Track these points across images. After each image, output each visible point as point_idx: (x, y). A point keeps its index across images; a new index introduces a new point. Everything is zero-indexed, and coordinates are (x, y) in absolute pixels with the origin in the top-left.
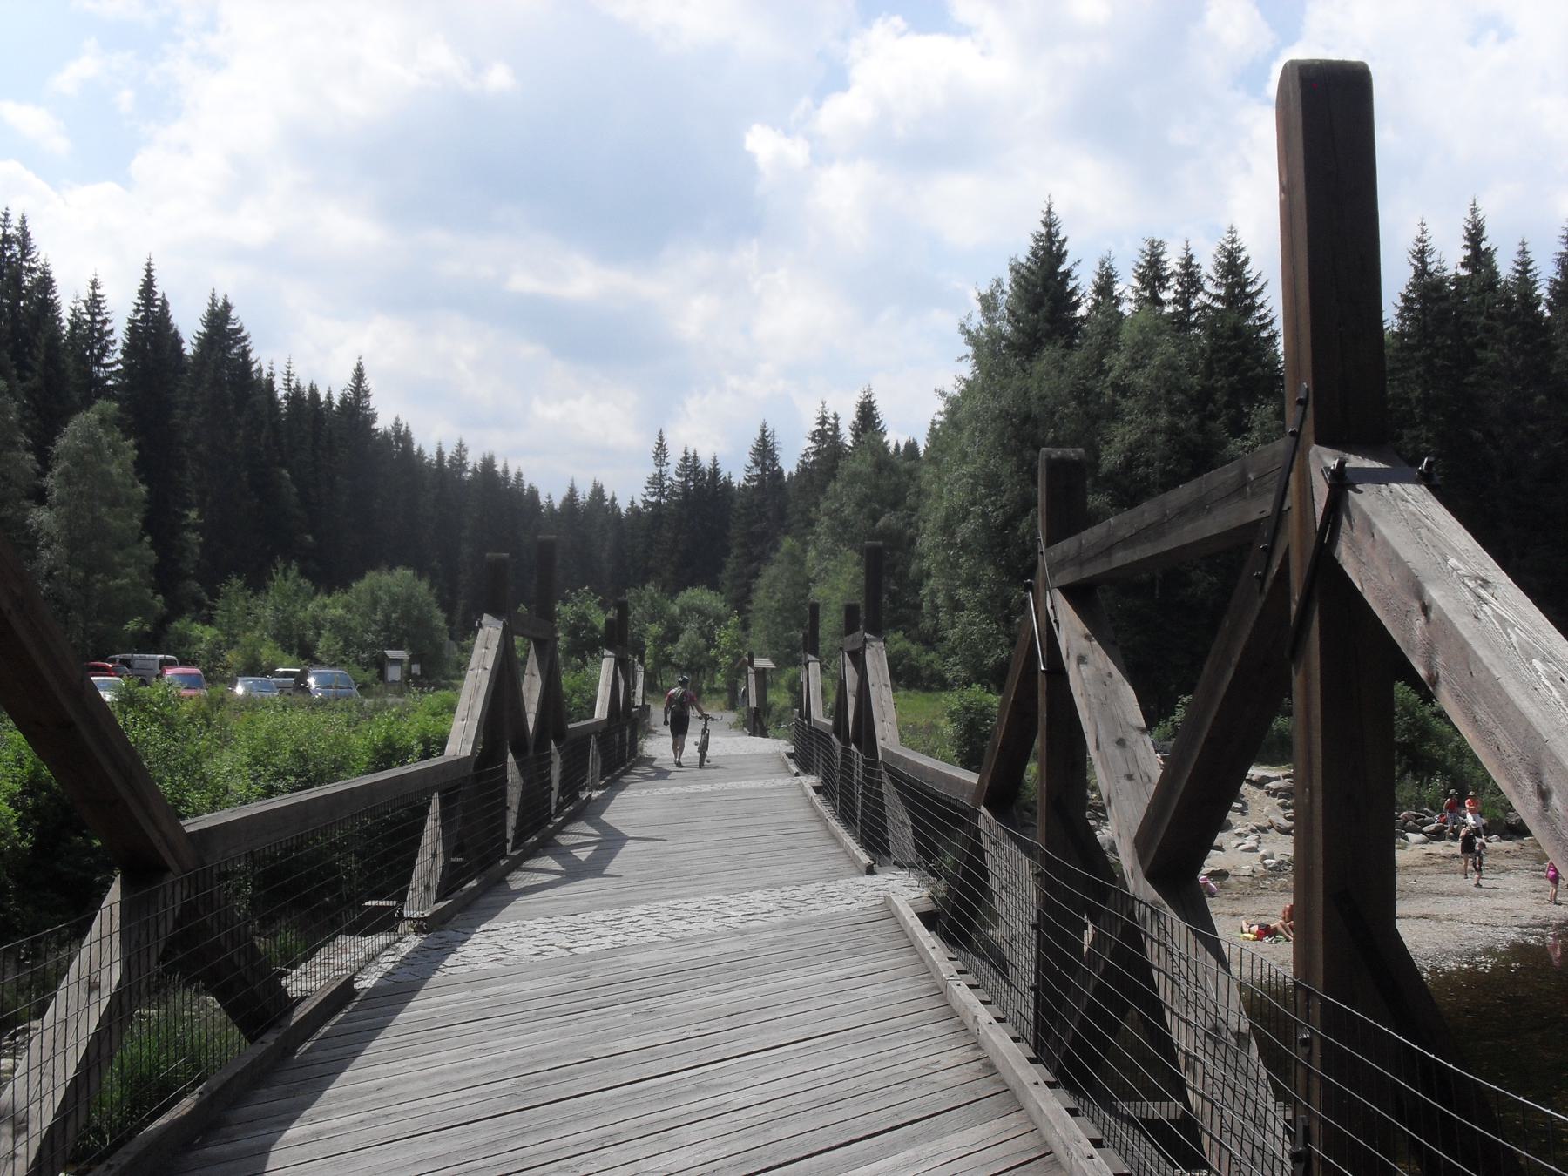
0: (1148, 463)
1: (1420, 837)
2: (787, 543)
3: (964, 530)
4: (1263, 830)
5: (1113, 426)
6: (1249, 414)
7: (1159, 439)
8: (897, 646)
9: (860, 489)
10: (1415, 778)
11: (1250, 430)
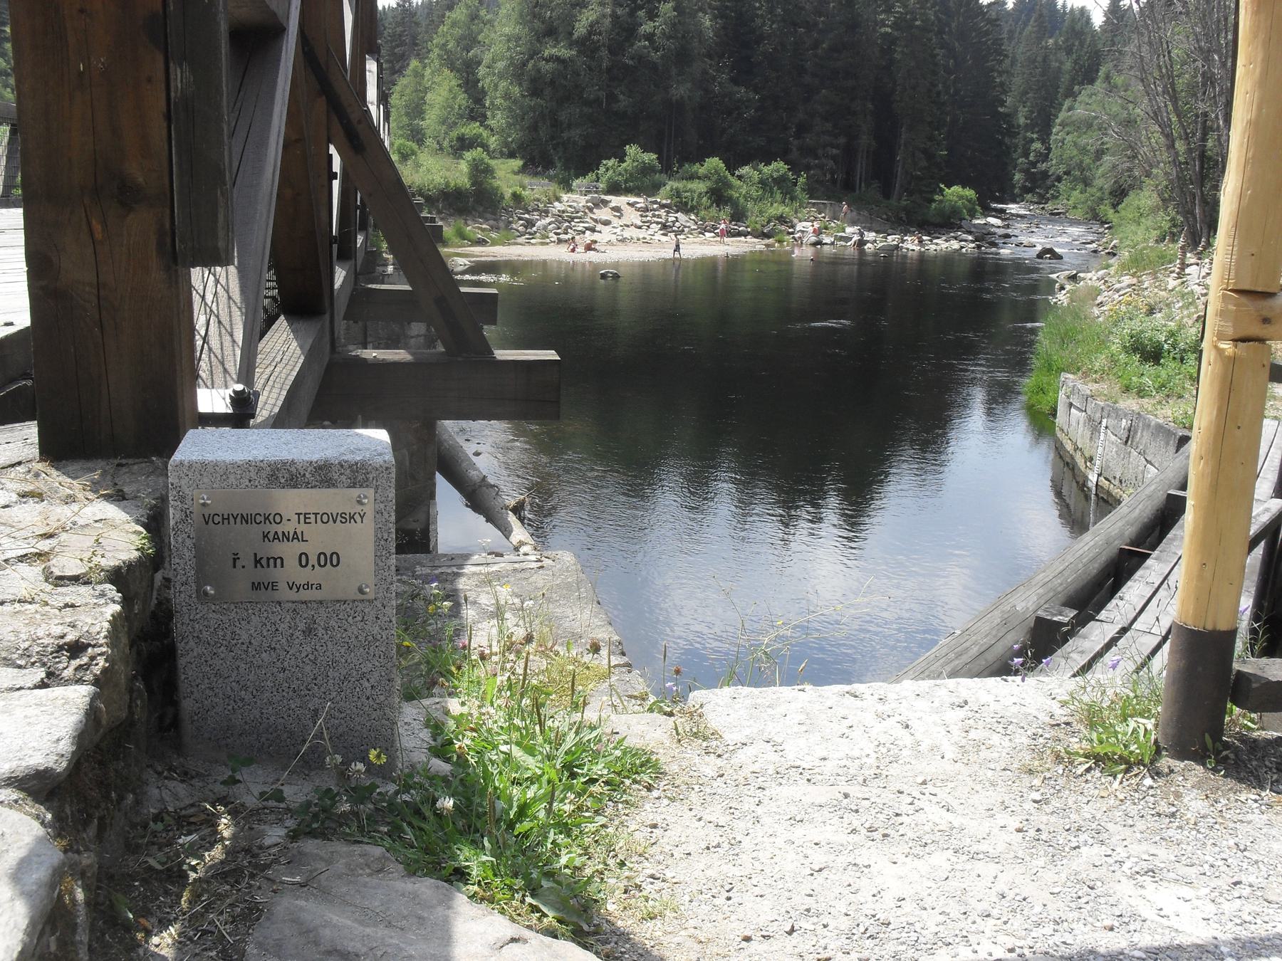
0: (600, 34)
1: (712, 234)
2: (414, 63)
3: (501, 65)
4: (628, 226)
5: (584, 10)
6: (658, 8)
7: (608, 21)
8: (474, 132)
9: (458, 32)
10: (718, 206)
11: (658, 16)
